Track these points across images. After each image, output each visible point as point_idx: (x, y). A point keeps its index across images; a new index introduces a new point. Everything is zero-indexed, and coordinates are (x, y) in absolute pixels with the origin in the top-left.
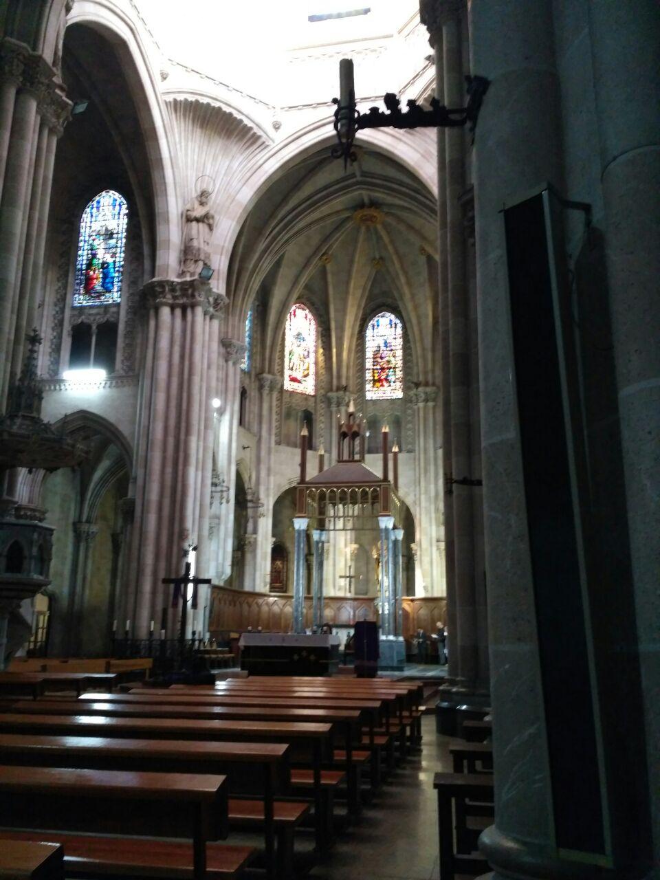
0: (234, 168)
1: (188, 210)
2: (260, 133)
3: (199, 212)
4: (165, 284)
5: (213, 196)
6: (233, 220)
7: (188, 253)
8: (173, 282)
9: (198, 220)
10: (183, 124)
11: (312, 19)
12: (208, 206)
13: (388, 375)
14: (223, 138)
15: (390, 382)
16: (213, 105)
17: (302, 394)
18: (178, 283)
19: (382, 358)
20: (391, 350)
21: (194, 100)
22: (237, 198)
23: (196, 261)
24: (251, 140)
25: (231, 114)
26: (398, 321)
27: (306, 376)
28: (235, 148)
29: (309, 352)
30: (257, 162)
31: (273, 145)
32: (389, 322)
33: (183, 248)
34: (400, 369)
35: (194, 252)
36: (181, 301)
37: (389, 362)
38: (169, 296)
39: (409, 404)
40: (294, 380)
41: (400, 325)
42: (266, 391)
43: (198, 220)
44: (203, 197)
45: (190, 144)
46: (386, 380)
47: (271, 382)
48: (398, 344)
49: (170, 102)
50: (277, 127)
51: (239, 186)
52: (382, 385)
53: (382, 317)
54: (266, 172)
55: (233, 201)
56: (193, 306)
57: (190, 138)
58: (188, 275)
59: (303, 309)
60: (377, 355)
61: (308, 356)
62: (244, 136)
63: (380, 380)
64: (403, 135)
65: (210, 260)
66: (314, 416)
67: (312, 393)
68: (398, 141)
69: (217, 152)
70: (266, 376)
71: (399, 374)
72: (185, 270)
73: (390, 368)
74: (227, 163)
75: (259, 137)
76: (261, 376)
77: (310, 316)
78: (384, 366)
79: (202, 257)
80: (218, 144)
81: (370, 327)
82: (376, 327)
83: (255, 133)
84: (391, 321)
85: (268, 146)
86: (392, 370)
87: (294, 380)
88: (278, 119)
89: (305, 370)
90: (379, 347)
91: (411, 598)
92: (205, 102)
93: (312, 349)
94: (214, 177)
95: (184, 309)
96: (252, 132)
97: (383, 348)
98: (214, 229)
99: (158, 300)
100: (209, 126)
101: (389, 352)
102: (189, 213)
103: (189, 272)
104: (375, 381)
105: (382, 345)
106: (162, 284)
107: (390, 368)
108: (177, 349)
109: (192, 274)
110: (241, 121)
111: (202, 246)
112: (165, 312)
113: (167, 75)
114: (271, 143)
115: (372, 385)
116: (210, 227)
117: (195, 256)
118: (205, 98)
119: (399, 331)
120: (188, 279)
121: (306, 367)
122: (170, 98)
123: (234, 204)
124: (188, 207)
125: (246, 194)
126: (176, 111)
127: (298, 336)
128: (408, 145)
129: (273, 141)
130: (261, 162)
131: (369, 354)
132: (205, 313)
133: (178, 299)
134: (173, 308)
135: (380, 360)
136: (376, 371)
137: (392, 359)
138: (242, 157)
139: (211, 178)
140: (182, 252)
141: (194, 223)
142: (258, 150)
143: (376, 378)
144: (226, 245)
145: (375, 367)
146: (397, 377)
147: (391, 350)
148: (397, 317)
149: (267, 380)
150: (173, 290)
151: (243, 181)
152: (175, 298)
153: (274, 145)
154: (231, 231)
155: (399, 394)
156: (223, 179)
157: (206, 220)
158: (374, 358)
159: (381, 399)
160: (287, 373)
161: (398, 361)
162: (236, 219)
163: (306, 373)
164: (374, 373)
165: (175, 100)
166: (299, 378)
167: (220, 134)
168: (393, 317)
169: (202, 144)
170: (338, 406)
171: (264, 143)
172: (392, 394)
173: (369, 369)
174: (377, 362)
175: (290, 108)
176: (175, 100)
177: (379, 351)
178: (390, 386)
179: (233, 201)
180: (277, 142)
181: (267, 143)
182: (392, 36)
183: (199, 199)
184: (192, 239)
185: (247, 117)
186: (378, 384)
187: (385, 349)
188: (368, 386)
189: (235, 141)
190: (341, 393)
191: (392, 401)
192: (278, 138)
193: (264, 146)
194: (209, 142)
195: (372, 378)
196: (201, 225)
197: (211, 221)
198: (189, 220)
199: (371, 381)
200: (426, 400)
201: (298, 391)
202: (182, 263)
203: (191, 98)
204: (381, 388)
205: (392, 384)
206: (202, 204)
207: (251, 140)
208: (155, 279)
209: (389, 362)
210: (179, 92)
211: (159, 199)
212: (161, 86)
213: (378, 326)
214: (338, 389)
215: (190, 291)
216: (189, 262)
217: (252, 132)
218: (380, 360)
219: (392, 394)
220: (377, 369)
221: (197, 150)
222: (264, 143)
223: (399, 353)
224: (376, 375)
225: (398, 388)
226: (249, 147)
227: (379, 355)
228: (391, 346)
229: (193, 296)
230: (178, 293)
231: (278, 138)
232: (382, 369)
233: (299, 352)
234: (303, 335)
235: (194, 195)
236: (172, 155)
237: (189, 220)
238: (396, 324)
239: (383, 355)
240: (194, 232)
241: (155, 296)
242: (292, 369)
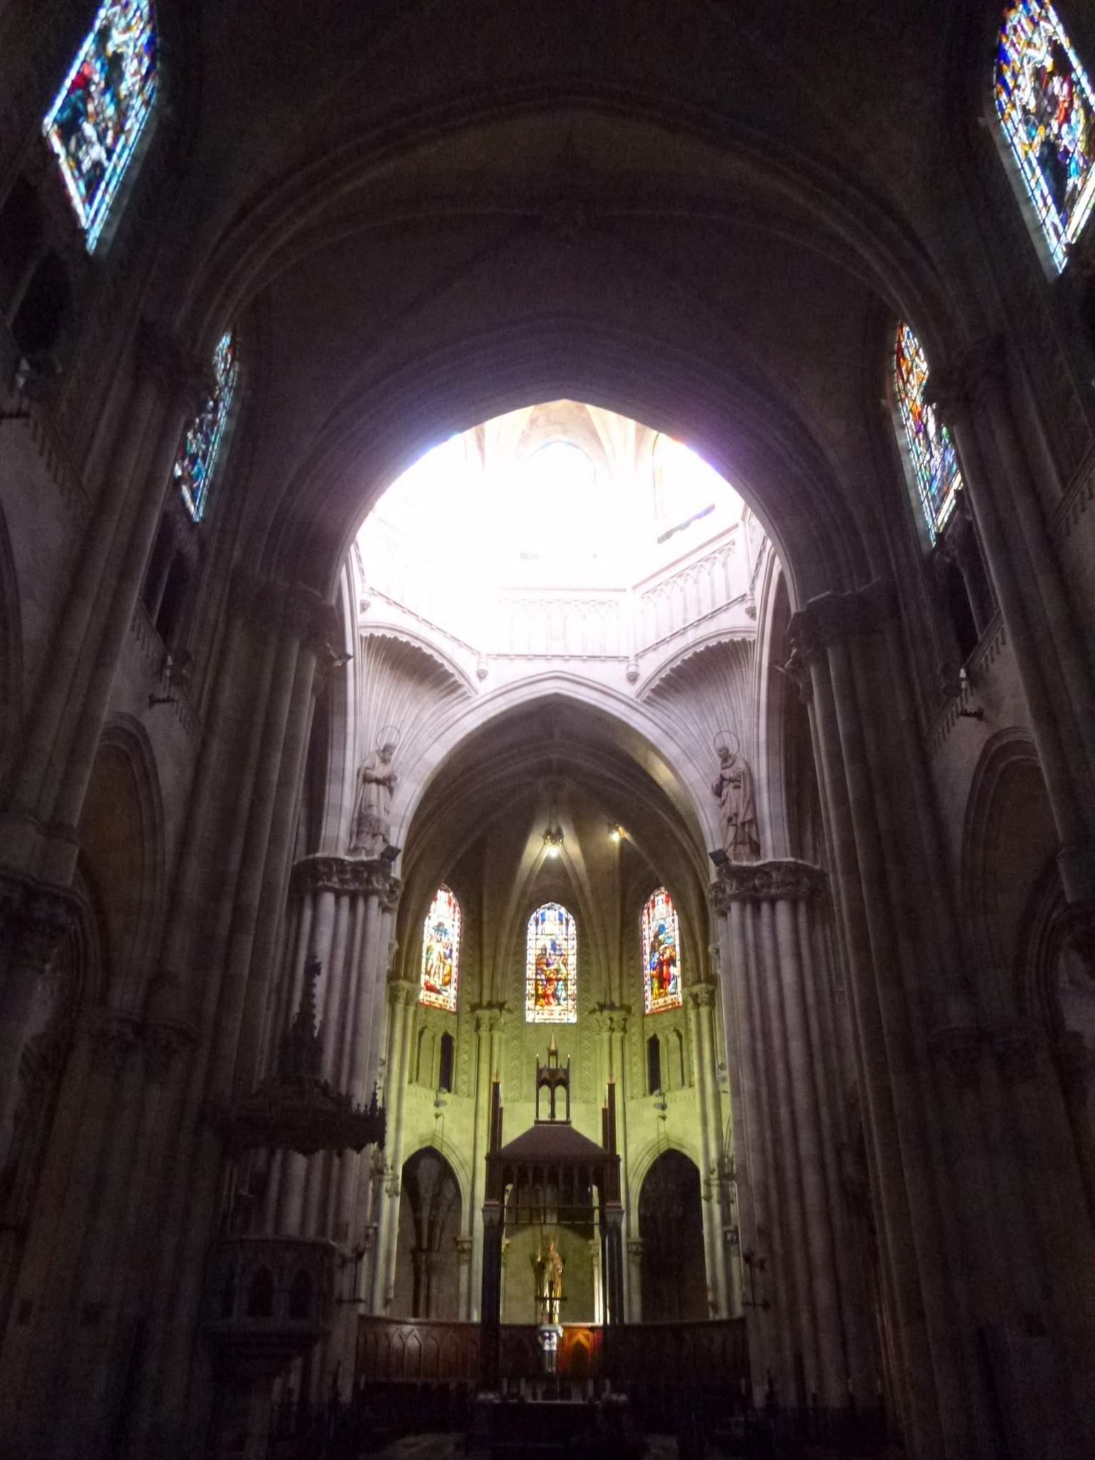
0: (425, 719)
1: (367, 768)
2: (461, 681)
3: (380, 771)
4: (332, 862)
5: (395, 753)
6: (419, 785)
7: (364, 823)
8: (342, 861)
9: (378, 782)
11: (524, 556)
12: (391, 764)
13: (556, 990)
15: (558, 999)
16: (413, 644)
17: (441, 1009)
18: (350, 863)
19: (548, 965)
20: (561, 955)
21: (392, 637)
22: (426, 756)
23: (374, 835)
24: (448, 690)
25: (431, 656)
26: (570, 917)
27: (447, 983)
28: (427, 695)
29: (451, 951)
30: (454, 715)
31: (475, 697)
32: (557, 917)
33: (356, 816)
34: (573, 982)
35: (373, 823)
36: (351, 887)
37: (557, 971)
38: (335, 879)
39: (587, 1033)
40: (431, 988)
41: (572, 922)
42: (400, 1007)
43: (378, 782)
44: (386, 753)
46: (555, 996)
47: (408, 992)
48: (571, 947)
50: (482, 675)
52: (549, 1003)
53: (549, 909)
54: (465, 728)
55: (420, 759)
56: (367, 896)
57: (377, 679)
58: (364, 852)
59: (446, 891)
60: (542, 961)
61: (450, 956)
63: (545, 996)
64: (640, 705)
65: (389, 834)
66: (455, 1044)
67: (454, 1010)
68: (634, 711)
69: (405, 698)
70: (404, 984)
71: (572, 989)
72: (360, 845)
73: (558, 980)
74: (416, 712)
75: (460, 686)
76: (393, 984)
77: (454, 901)
78: (552, 975)
79: (382, 829)
80: (407, 688)
81: (532, 921)
82: (540, 922)
83: (456, 682)
84: (561, 915)
86: (561, 983)
87: (431, 988)
88: (483, 667)
89: (445, 976)
90: (546, 950)
91: (590, 1324)
92: (405, 640)
93: (456, 946)
94: (398, 727)
95: (353, 898)
96: (453, 680)
97: (548, 951)
98: (395, 792)
99: (320, 883)
101: (558, 958)
102: (369, 772)
103: (363, 848)
104: (538, 997)
105: (549, 946)
106: (328, 862)
107: (558, 980)
108: (341, 952)
109: (369, 852)
110: (442, 665)
111: (383, 815)
112: (328, 900)
113: (368, 605)
115: (533, 1001)
116: (391, 790)
117: (374, 828)
118: (404, 636)
119: (572, 929)
120: (364, 858)
121: (447, 968)
122: (366, 633)
123: (421, 762)
124: (367, 763)
125: (437, 754)
126: (369, 648)
127: (440, 928)
128: (646, 716)
129: (477, 693)
130: (459, 716)
131: (531, 958)
132: (380, 904)
133: (347, 884)
134: (338, 895)
135: (545, 968)
136: (540, 983)
137: (562, 967)
138: (434, 709)
139: (395, 728)
140: (355, 822)
141: (374, 786)
142: (455, 702)
143: (540, 992)
145: (539, 977)
146: (569, 993)
147: (561, 955)
148: (569, 910)
149: (404, 988)
150: (342, 871)
152: (342, 881)
153: (478, 697)
154: (415, 798)
155: (573, 1018)
156: (408, 732)
157: (387, 783)
158: (536, 964)
159: (547, 1022)
160: (424, 978)
161: (571, 970)
162: (422, 784)
163: (447, 979)
164: (537, 985)
165: (372, 636)
166: (438, 987)
168: (563, 910)
170: (490, 1030)
171: (465, 693)
172: (562, 1017)
173: (530, 980)
174: (542, 970)
175: (499, 655)
176: (372, 636)
177: (546, 954)
178: (559, 1004)
179: (420, 759)
180: (481, 693)
181: (470, 695)
182: (625, 590)
183: (381, 755)
184: (370, 806)
185: (450, 662)
186: (542, 1001)
187: (552, 952)
188: (530, 1003)
190: (496, 1011)
191: (563, 1026)
192: (485, 688)
194: (397, 685)
195: (533, 992)
196: (381, 787)
198: (367, 780)
199: (533, 995)
200: (612, 1030)
201: (437, 1005)
202: (354, 837)
203: (390, 635)
204: (546, 1007)
205: (561, 1001)
206: (385, 761)
207: (448, 690)
208: (318, 855)
209: (557, 971)
210: (377, 627)
211: (335, 751)
212: (361, 618)
213: (543, 920)
214: (490, 1006)
215: (365, 875)
216: (364, 835)
217: (453, 680)
218: (545, 968)
219: (562, 1017)
220: (542, 980)
221: (382, 694)
223: (573, 960)
224: (540, 988)
225: (570, 1007)
226: (445, 696)
227: (545, 961)
228: (560, 949)
229: (369, 881)
230: (348, 876)
231: (485, 688)
232: (549, 980)
233: (438, 949)
234: (446, 927)
235: (373, 748)
236: (358, 699)
237: (367, 780)
238: (567, 921)
239: (550, 961)
240: (374, 797)
241: (316, 879)
242: (428, 973)
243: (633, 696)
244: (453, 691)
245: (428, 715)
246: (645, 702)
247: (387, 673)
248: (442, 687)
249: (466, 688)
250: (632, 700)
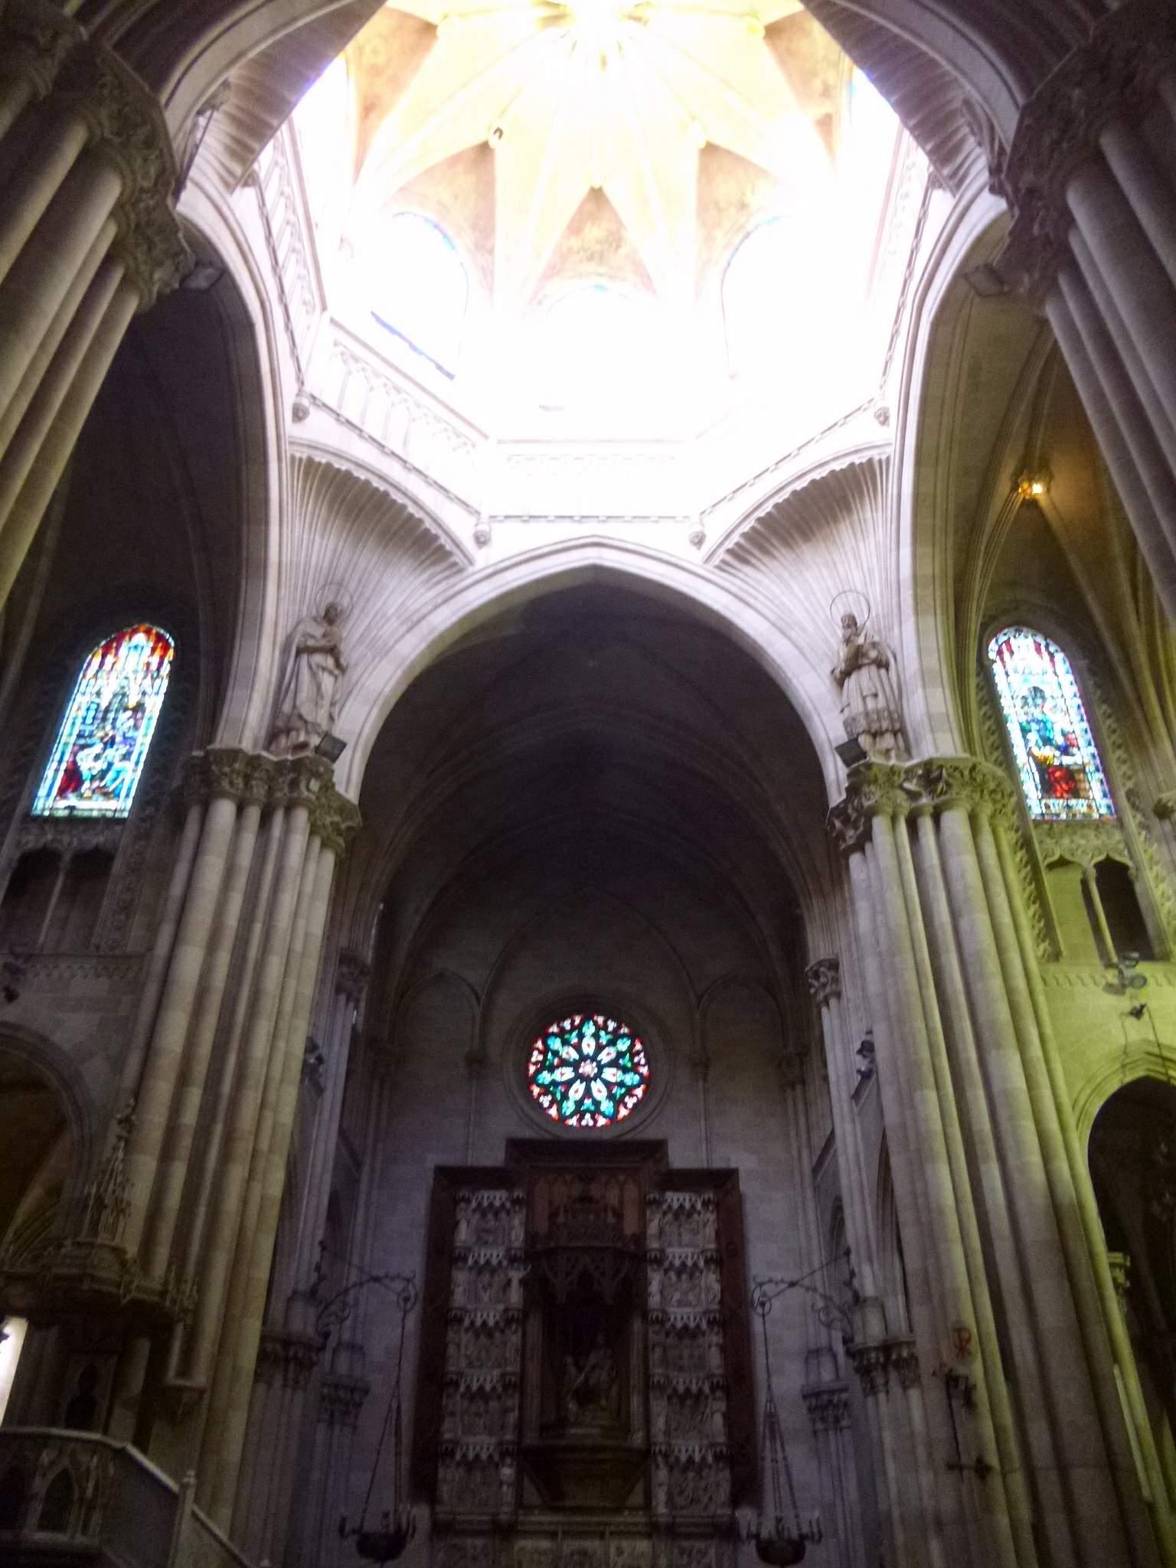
1: (833, 672)
9: (847, 674)
49: (723, 561)
51: (894, 558)
62: (859, 485)
85: (888, 460)
100: (814, 528)
151: (894, 546)
167: (835, 520)
171: (880, 461)
176: (730, 551)
180: (893, 441)
181: (884, 457)
189: (857, 501)
222: (880, 461)
247: (806, 550)
249: (875, 454)
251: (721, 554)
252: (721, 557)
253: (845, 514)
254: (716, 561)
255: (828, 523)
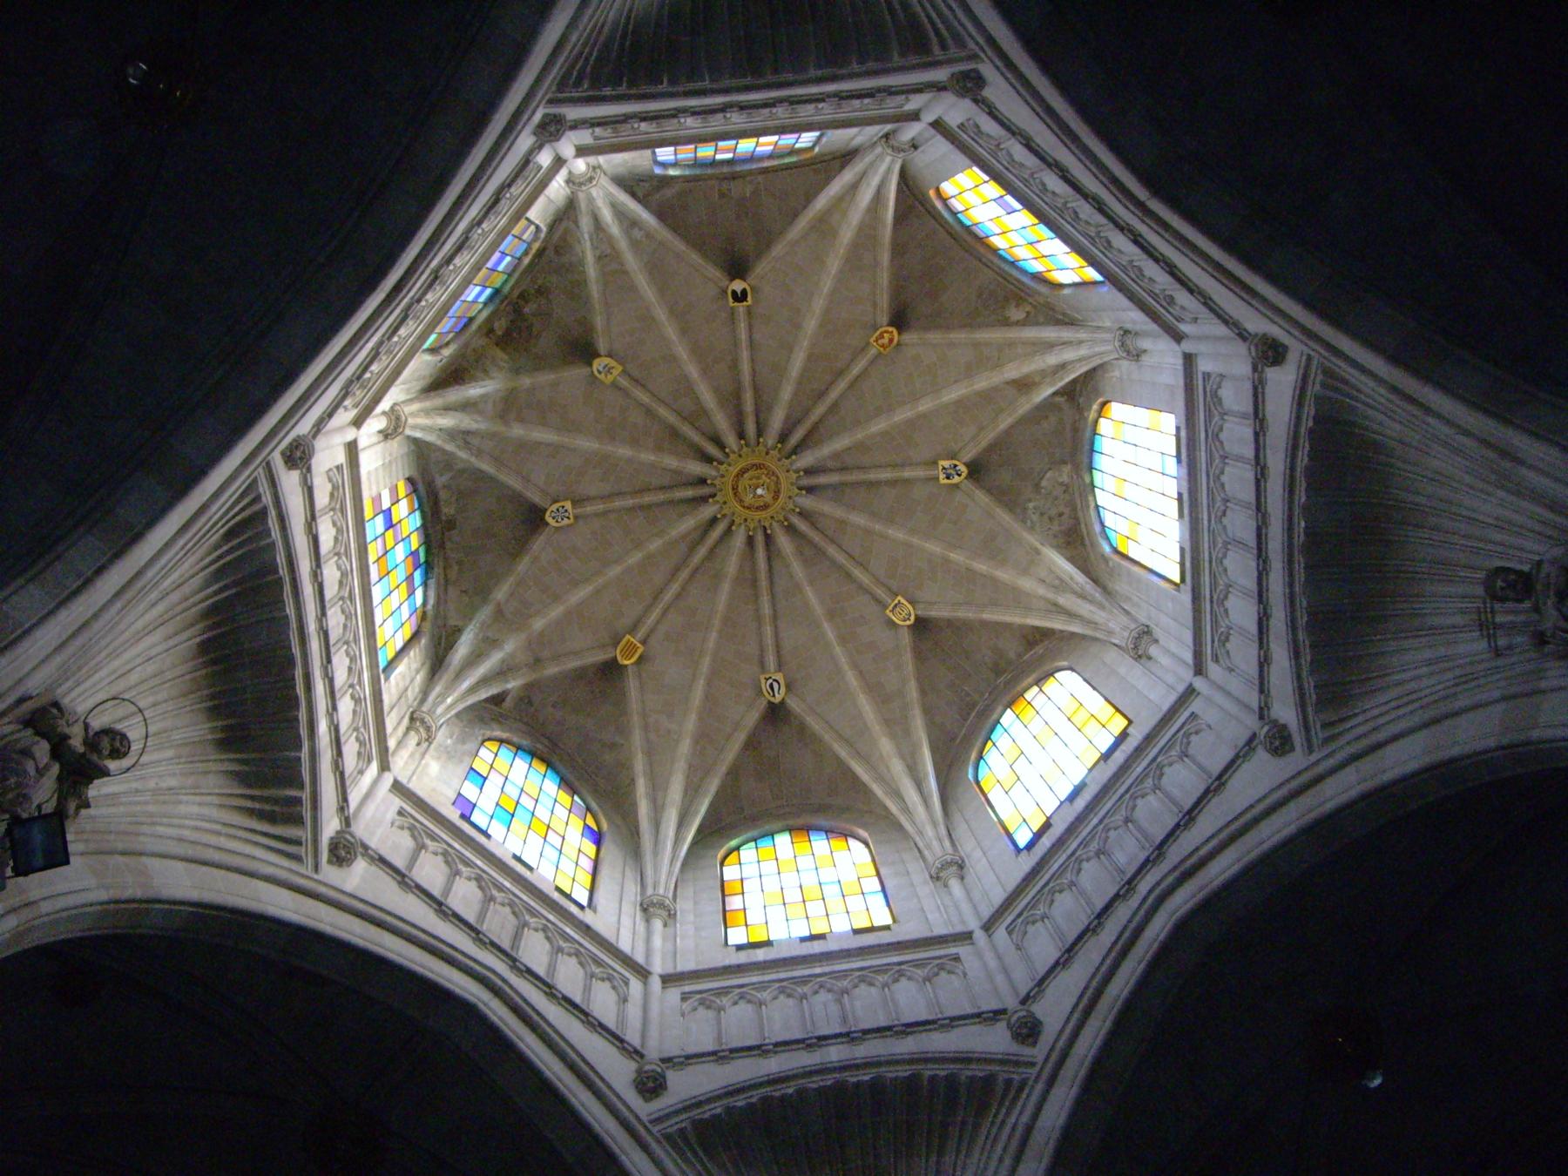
0: (182, 809)
1: (56, 705)
9: (59, 747)
10: (197, 581)
14: (213, 730)
43: (59, 747)
45: (157, 636)
49: (258, 499)
57: (169, 628)
62: (263, 782)
64: (659, 1142)
74: (173, 782)
75: (298, 820)
83: (298, 801)
114: (310, 861)
138: (215, 813)
144: (45, 907)
151: (190, 851)
167: (214, 712)
169: (169, 675)
171: (298, 843)
193: (290, 848)
197: (72, 806)
221: (151, 668)
226: (251, 812)
243: (645, 1119)
244: (271, 818)
245: (195, 809)
246: (668, 1137)
247: (189, 640)
248: (256, 792)
250: (637, 1118)
251: (267, 499)
252: (264, 499)
253: (219, 736)
254: (264, 488)
255: (212, 697)
